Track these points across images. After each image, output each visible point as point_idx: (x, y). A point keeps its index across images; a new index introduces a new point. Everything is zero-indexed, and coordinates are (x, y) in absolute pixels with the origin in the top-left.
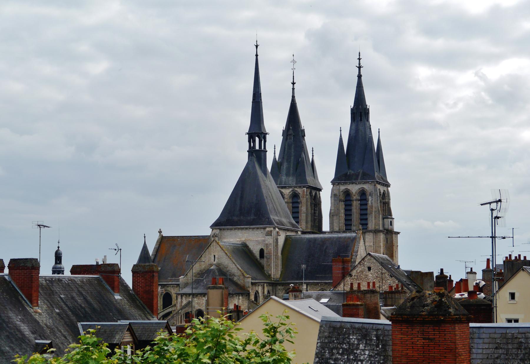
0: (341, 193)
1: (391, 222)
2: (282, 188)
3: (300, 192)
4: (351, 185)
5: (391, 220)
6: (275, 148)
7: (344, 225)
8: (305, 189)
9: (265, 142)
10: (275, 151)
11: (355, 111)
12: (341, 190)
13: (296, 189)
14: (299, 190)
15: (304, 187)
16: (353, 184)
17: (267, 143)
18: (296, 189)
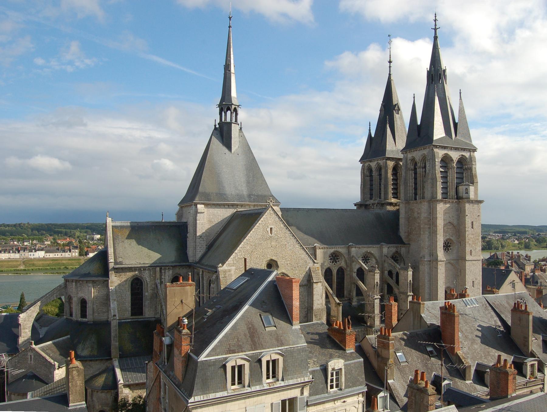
0: (410, 161)
1: (466, 189)
2: (370, 162)
3: (382, 165)
4: (415, 152)
5: (467, 187)
6: (370, 125)
7: (414, 195)
8: (384, 160)
9: (237, 114)
10: (370, 128)
11: (433, 73)
12: (409, 159)
13: (379, 162)
14: (381, 162)
15: (384, 159)
16: (416, 150)
17: (238, 116)
18: (379, 162)
